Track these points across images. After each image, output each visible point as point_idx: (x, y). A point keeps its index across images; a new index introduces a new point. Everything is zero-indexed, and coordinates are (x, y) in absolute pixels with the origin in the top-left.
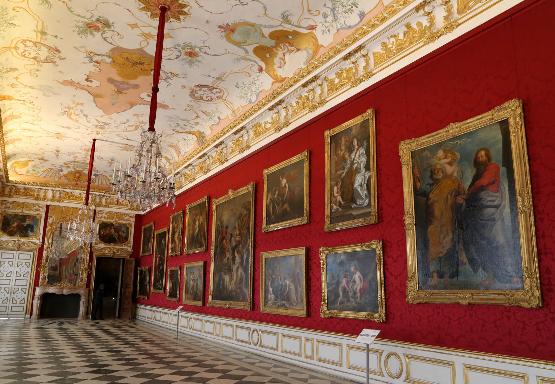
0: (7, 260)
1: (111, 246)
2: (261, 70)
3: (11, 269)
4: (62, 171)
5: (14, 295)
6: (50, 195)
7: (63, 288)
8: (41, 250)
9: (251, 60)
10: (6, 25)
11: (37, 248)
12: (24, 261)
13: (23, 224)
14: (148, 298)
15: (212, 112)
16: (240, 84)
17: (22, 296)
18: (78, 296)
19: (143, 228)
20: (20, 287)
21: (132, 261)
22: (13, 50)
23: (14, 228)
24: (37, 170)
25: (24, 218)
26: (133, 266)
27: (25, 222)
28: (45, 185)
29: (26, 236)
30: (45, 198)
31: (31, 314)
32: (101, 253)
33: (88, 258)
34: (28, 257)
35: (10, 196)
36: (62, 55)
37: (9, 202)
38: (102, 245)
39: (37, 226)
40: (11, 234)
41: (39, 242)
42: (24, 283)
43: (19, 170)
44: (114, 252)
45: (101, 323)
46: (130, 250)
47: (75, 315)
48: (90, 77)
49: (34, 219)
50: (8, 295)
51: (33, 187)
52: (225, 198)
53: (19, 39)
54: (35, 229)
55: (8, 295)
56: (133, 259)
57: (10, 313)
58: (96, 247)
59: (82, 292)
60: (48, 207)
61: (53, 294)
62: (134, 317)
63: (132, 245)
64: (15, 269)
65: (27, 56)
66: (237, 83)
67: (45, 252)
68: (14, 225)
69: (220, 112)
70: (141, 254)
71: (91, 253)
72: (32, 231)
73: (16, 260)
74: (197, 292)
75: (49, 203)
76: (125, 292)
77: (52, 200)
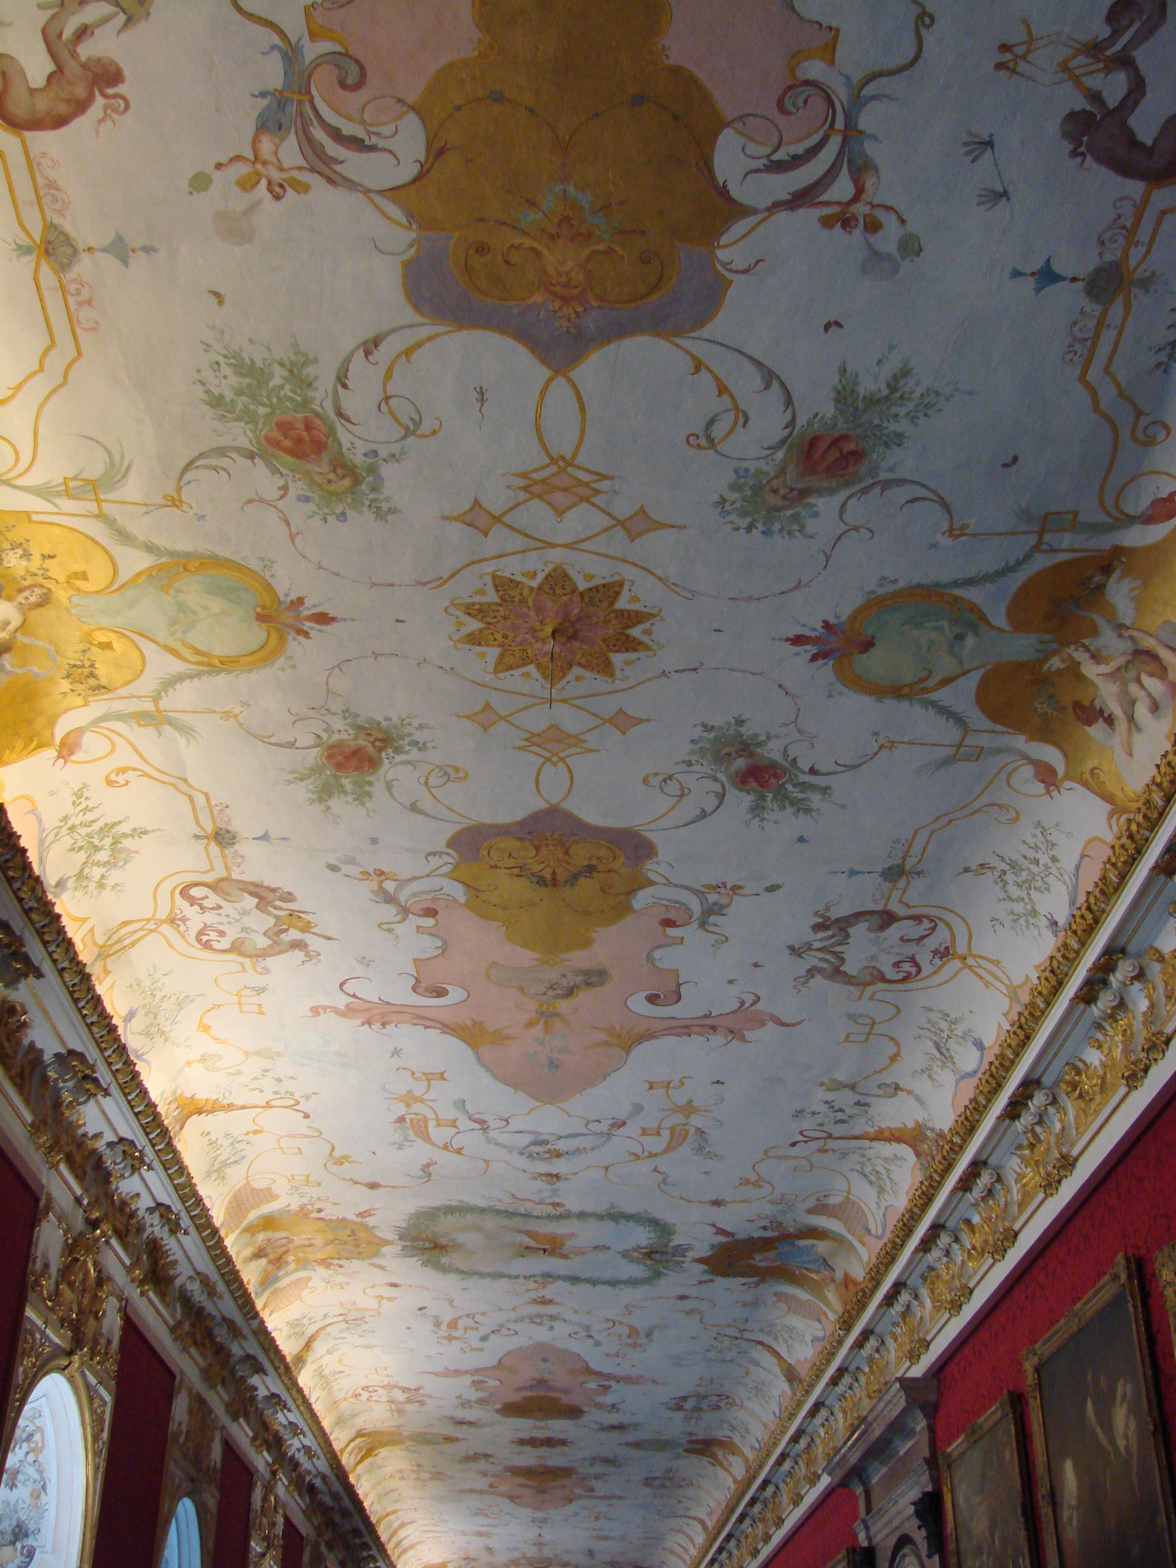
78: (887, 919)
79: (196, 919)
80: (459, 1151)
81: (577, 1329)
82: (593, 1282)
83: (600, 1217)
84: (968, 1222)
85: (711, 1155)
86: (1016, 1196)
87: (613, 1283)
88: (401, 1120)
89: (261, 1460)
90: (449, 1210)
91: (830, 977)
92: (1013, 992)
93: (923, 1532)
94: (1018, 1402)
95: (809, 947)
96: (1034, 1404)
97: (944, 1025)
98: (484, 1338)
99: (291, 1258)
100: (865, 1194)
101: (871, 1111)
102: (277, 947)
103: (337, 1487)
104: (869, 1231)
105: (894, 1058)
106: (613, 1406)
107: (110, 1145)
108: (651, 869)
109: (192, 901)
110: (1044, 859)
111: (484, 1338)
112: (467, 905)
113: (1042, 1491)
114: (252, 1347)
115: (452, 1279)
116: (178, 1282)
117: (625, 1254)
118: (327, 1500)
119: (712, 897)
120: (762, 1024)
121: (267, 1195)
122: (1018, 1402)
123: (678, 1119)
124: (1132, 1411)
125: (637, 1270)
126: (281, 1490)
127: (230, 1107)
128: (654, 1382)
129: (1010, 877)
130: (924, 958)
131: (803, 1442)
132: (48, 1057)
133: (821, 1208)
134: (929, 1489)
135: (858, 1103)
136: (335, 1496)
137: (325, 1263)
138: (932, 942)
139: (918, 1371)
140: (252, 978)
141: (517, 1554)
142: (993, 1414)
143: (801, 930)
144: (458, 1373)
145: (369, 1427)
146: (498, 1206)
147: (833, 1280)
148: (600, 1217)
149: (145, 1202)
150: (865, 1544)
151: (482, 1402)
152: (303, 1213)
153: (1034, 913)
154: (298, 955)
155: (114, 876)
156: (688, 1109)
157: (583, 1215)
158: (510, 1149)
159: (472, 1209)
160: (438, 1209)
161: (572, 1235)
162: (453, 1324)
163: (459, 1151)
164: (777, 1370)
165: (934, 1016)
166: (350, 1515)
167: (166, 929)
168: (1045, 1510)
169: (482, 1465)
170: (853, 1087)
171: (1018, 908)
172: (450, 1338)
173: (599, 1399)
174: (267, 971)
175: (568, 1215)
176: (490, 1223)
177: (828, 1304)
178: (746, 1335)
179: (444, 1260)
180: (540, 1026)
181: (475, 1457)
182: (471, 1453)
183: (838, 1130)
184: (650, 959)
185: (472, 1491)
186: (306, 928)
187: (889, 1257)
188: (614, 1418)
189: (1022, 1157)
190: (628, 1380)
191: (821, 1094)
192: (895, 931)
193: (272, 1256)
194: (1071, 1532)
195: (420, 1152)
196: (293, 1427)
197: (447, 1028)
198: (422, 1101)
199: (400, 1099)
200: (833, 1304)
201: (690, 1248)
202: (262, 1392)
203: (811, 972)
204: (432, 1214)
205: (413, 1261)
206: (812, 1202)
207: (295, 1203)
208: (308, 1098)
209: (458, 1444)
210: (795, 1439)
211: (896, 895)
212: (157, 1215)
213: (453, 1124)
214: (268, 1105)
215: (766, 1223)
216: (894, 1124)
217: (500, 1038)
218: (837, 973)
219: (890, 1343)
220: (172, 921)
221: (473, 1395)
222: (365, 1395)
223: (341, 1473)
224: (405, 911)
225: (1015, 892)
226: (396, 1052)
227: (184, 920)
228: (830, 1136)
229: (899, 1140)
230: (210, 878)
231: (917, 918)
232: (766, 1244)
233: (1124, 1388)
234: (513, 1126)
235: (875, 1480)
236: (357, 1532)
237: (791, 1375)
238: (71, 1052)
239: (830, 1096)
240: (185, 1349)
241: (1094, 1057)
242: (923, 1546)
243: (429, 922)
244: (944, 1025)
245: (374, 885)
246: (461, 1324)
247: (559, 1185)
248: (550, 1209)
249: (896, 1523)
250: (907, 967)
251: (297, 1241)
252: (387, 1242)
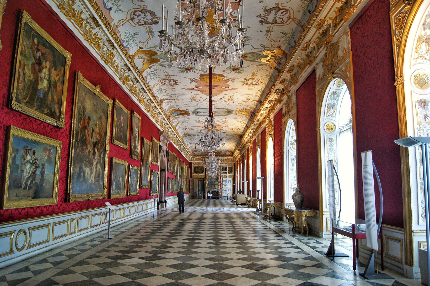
2: (140, 48)
9: (150, 48)
10: (287, 36)
15: (119, 4)
16: (136, 36)
22: (292, 17)
36: (259, 19)
48: (237, 4)
52: (91, 87)
53: (284, 24)
65: (284, 10)
66: (138, 35)
69: (116, 12)
74: (42, 185)
81: (206, 100)
82: (204, 108)
87: (201, 109)
98: (224, 97)
106: (192, 82)
111: (224, 97)
125: (198, 111)
128: (185, 89)
144: (232, 89)
162: (229, 100)
204: (227, 115)
221: (230, 83)
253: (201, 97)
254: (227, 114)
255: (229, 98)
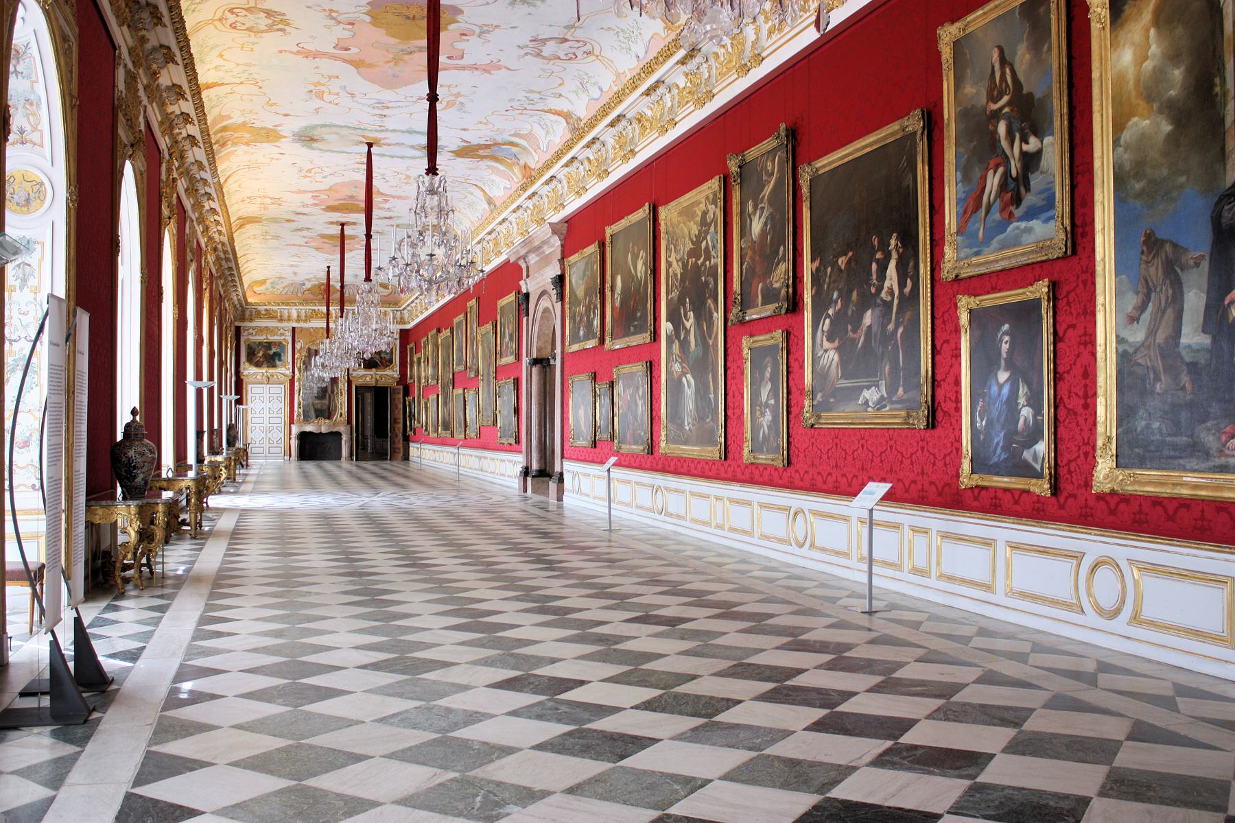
0: (258, 396)
1: (373, 371)
3: (263, 405)
4: (304, 284)
5: (270, 435)
6: (294, 314)
7: (320, 426)
8: (292, 382)
11: (288, 379)
12: (275, 396)
13: (269, 352)
14: (415, 434)
17: (278, 435)
18: (338, 434)
19: (408, 347)
20: (275, 426)
21: (399, 389)
23: (260, 357)
24: (277, 287)
25: (269, 345)
26: (401, 396)
27: (271, 349)
28: (288, 304)
29: (274, 366)
30: (289, 319)
31: (290, 456)
32: (360, 382)
33: (346, 389)
34: (280, 391)
35: (251, 320)
37: (250, 327)
38: (362, 372)
39: (284, 353)
40: (258, 365)
41: (289, 372)
42: (279, 421)
43: (257, 289)
44: (377, 380)
45: (363, 464)
46: (396, 376)
47: (338, 457)
49: (280, 344)
50: (263, 435)
51: (275, 308)
54: (282, 358)
55: (263, 435)
56: (401, 387)
57: (268, 455)
58: (355, 374)
59: (342, 429)
60: (294, 329)
61: (310, 432)
62: (406, 457)
63: (398, 368)
64: (267, 405)
67: (296, 384)
68: (260, 354)
70: (409, 381)
71: (349, 382)
72: (280, 360)
73: (266, 395)
75: (295, 325)
76: (394, 428)
77: (299, 319)
78: (566, 40)
79: (232, 18)
80: (337, 104)
82: (392, 157)
83: (403, 132)
84: (588, 158)
85: (464, 112)
86: (611, 156)
87: (402, 157)
88: (311, 91)
89: (203, 241)
90: (325, 126)
91: (535, 56)
92: (618, 75)
93: (555, 291)
94: (602, 245)
95: (527, 46)
96: (608, 249)
97: (585, 77)
98: (324, 177)
99: (229, 143)
100: (539, 133)
101: (547, 102)
102: (270, 29)
103: (229, 249)
104: (540, 148)
105: (560, 85)
107: (177, 116)
108: (459, 18)
109: (233, 13)
110: (636, 32)
111: (324, 177)
112: (370, 23)
113: (608, 285)
114: (211, 191)
115: (316, 153)
116: (186, 165)
117: (413, 147)
118: (222, 255)
119: (485, 28)
120: (500, 69)
121: (229, 117)
122: (602, 245)
123: (454, 98)
124: (645, 263)
126: (209, 256)
127: (222, 84)
129: (621, 34)
130: (579, 53)
131: (493, 235)
132: (163, 87)
133: (516, 135)
134: (559, 273)
135: (541, 98)
136: (225, 252)
137: (247, 144)
138: (584, 49)
139: (557, 217)
140: (253, 39)
141: (311, 276)
142: (593, 249)
143: (525, 40)
144: (305, 192)
145: (245, 215)
146: (350, 125)
147: (518, 164)
148: (403, 132)
149: (184, 134)
150: (524, 291)
151: (316, 205)
152: (244, 124)
153: (630, 50)
154: (281, 33)
155: (200, 7)
156: (458, 95)
157: (394, 131)
158: (364, 105)
159: (336, 126)
160: (318, 125)
161: (385, 139)
162: (309, 171)
163: (337, 104)
164: (482, 198)
165: (581, 73)
166: (230, 261)
167: (217, 23)
168: (608, 293)
169: (305, 233)
170: (539, 93)
171: (623, 45)
172: (305, 177)
173: (381, 205)
174: (261, 37)
175: (387, 130)
176: (344, 132)
177: (515, 174)
178: (468, 181)
179: (315, 145)
180: (393, 63)
181: (302, 229)
182: (300, 227)
183: (529, 107)
184: (452, 45)
185: (294, 245)
186: (288, 24)
187: (548, 165)
188: (387, 214)
189: (615, 140)
190: (399, 197)
191: (524, 94)
192: (567, 44)
193: (221, 143)
194: (617, 304)
195: (317, 103)
196: (218, 223)
197: (345, 61)
198: (323, 85)
199: (313, 84)
200: (517, 177)
201: (447, 146)
202: (207, 207)
203: (526, 54)
204: (314, 127)
205: (298, 145)
206: (513, 132)
207: (240, 120)
208: (263, 81)
209: (292, 223)
210: (489, 233)
211: (569, 34)
212: (188, 141)
213: (337, 94)
214: (241, 83)
215: (488, 139)
216: (558, 108)
217: (371, 66)
218: (539, 55)
219: (545, 199)
220: (220, 20)
222: (249, 200)
223: (231, 240)
224: (340, 22)
225: (623, 40)
226: (317, 67)
227: (226, 19)
228: (525, 109)
229: (559, 115)
230: (246, 7)
231: (579, 41)
232: (487, 147)
233: (642, 254)
234: (368, 96)
235: (532, 262)
236: (230, 269)
237: (490, 202)
238: (174, 85)
239: (527, 95)
240: (189, 199)
241: (649, 113)
242: (554, 297)
243: (351, 27)
244: (585, 77)
245: (328, 14)
246: (313, 171)
247: (384, 119)
248: (378, 128)
249: (542, 284)
250: (571, 56)
251: (236, 135)
252: (285, 137)
253: (387, 181)
254: (316, 133)
255: (308, 174)
